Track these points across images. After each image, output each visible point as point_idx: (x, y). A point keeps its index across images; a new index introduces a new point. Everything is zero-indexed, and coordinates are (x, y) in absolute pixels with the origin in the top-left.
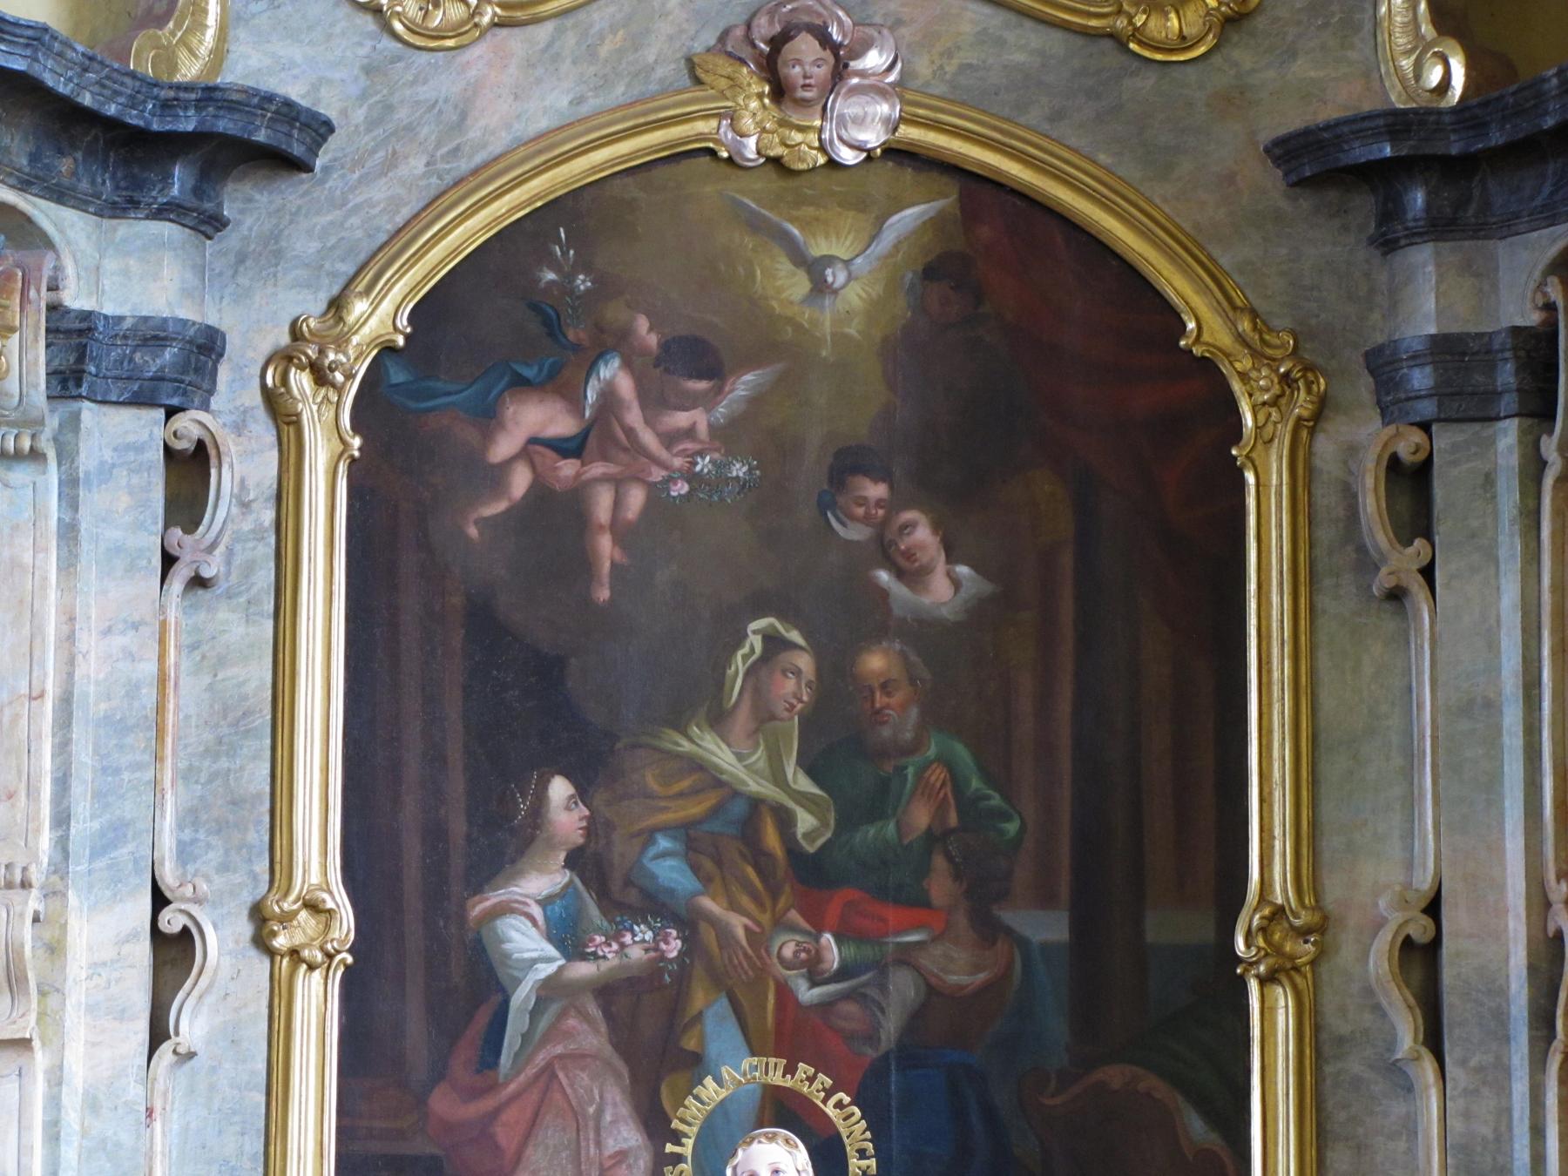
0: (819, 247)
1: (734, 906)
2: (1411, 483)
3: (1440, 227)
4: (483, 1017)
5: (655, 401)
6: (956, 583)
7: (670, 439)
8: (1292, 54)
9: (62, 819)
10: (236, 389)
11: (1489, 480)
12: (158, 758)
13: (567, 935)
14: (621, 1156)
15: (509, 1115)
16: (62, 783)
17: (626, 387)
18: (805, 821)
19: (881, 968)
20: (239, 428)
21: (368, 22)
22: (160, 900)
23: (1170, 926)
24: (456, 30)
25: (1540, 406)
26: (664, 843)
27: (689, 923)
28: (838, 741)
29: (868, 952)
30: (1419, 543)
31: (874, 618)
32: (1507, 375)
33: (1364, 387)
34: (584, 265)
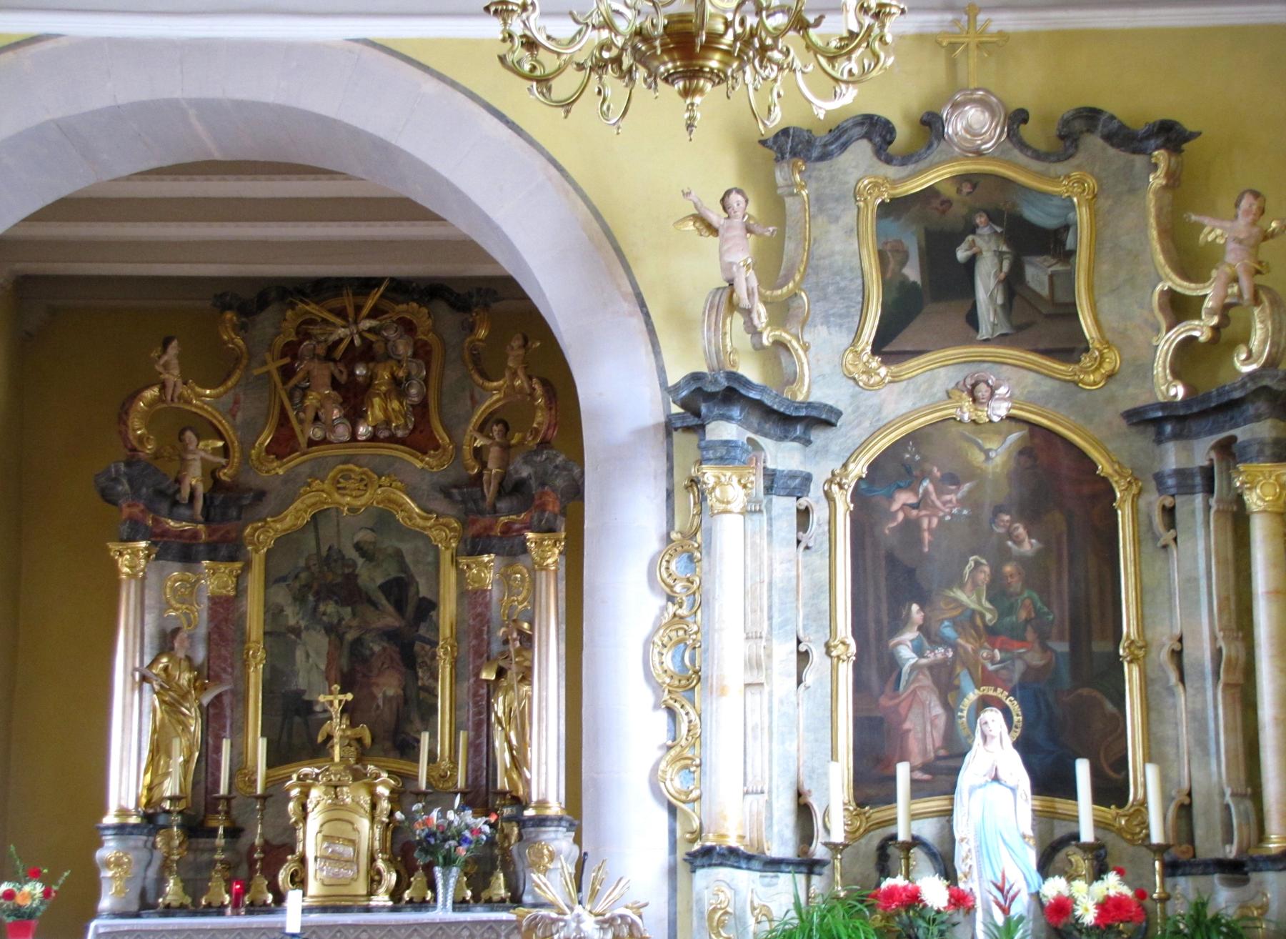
0: (988, 446)
1: (967, 641)
2: (1169, 512)
3: (1176, 436)
4: (894, 676)
5: (940, 493)
6: (1032, 545)
7: (944, 503)
8: (1128, 386)
9: (770, 618)
10: (816, 491)
11: (1193, 512)
12: (797, 600)
13: (919, 651)
14: (937, 716)
15: (903, 704)
16: (770, 608)
17: (931, 488)
18: (988, 616)
19: (1013, 659)
20: (817, 502)
21: (851, 382)
22: (799, 642)
23: (1099, 646)
24: (878, 384)
25: (1209, 490)
26: (946, 623)
27: (955, 647)
28: (998, 592)
29: (1009, 655)
30: (1172, 531)
31: (1005, 555)
32: (1198, 480)
33: (1153, 485)
34: (918, 452)
